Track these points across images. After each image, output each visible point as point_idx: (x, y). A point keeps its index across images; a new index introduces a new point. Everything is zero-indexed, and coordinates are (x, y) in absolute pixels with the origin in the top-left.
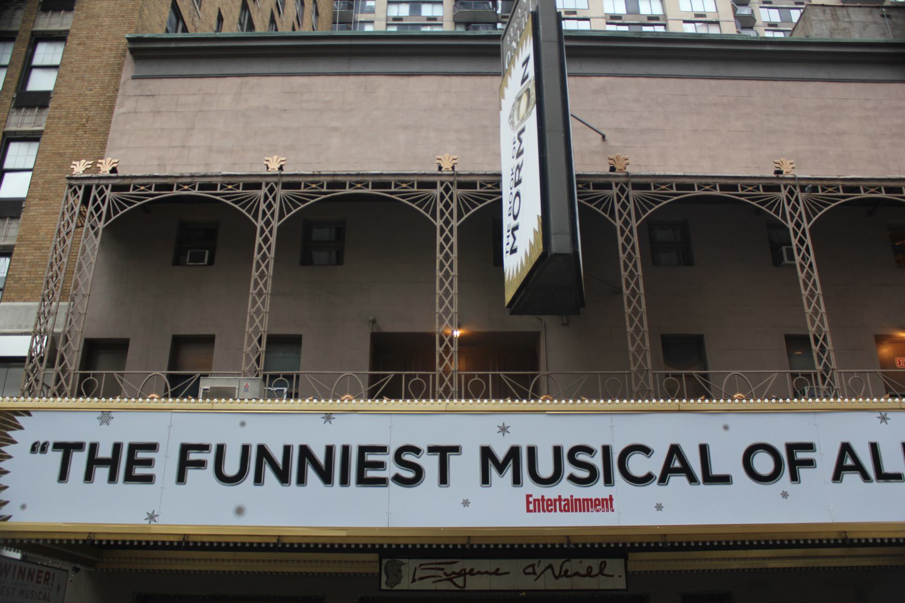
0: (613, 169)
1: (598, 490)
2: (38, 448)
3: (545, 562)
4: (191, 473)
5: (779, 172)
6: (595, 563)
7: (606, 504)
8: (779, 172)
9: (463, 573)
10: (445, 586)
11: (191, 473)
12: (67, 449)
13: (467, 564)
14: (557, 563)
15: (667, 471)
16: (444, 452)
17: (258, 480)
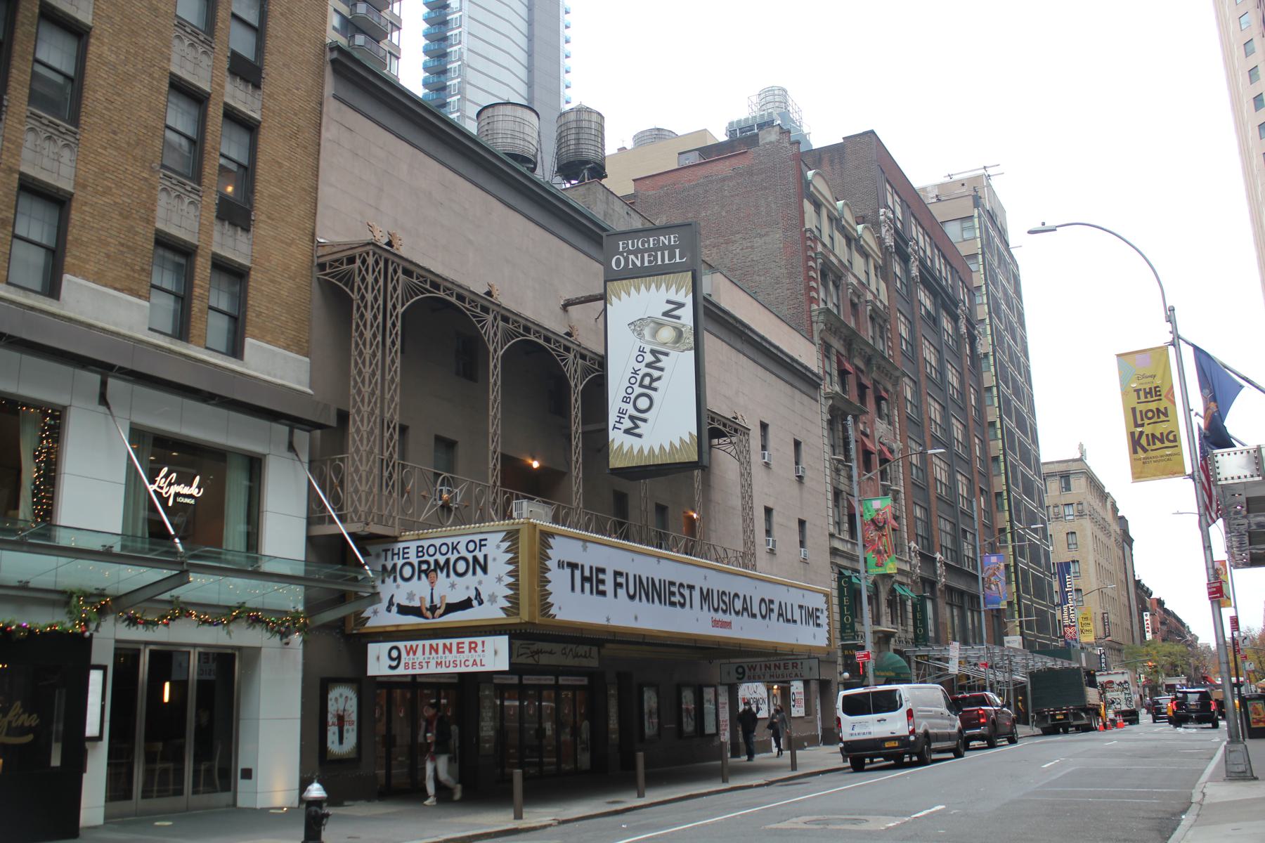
0: (390, 244)
1: (726, 618)
2: (561, 565)
3: (570, 646)
4: (619, 591)
5: (489, 293)
6: (586, 648)
7: (727, 625)
8: (489, 293)
9: (539, 652)
10: (530, 661)
11: (619, 591)
12: (573, 566)
13: (539, 645)
14: (574, 646)
15: (745, 609)
16: (691, 588)
17: (474, 573)
